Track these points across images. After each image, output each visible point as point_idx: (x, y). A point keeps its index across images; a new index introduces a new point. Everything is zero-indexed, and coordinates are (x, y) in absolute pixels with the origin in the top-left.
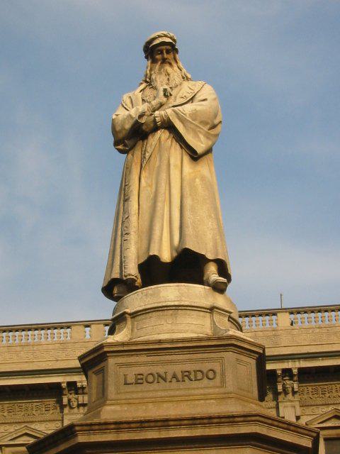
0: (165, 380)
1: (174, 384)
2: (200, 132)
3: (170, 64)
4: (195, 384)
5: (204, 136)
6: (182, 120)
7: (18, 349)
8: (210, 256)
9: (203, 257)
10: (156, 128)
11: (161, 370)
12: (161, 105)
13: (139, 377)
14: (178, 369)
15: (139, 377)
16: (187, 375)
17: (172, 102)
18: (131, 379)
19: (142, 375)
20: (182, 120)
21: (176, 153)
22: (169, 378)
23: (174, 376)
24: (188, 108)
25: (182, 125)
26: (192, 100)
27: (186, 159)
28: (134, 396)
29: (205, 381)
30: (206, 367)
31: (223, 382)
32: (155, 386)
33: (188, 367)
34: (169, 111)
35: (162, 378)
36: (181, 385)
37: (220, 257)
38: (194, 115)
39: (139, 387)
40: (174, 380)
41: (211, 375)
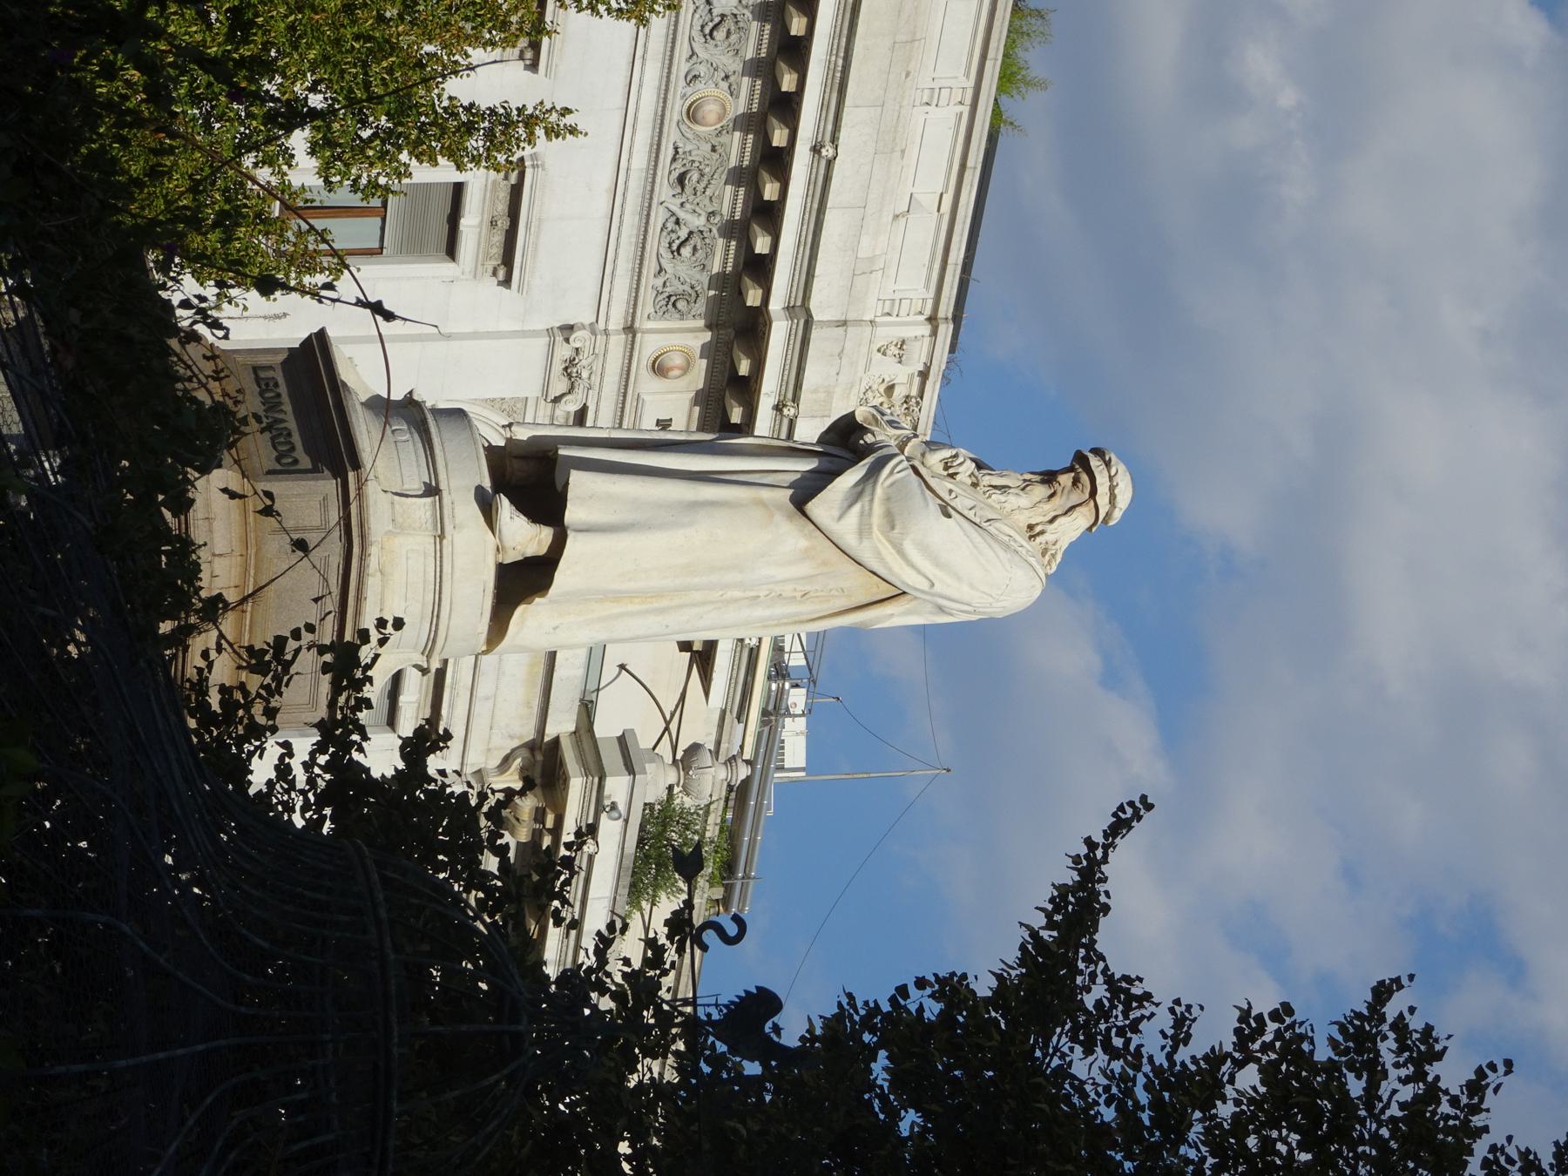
18: (262, 375)
29: (275, 454)
31: (269, 472)
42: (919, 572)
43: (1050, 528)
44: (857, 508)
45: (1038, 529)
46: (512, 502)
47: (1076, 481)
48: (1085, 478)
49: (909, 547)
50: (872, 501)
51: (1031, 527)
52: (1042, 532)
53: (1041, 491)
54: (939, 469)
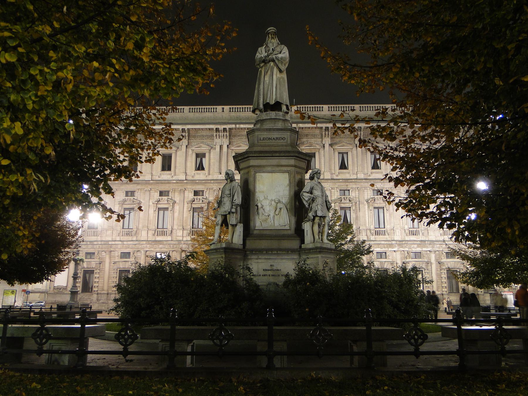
1: (274, 141)
4: (279, 141)
6: (278, 60)
10: (269, 61)
12: (271, 53)
14: (275, 137)
16: (277, 138)
17: (275, 52)
18: (262, 139)
20: (278, 60)
21: (275, 70)
23: (274, 138)
24: (280, 56)
26: (280, 53)
27: (278, 72)
32: (268, 141)
34: (274, 57)
36: (276, 141)
38: (282, 58)
39: (264, 141)
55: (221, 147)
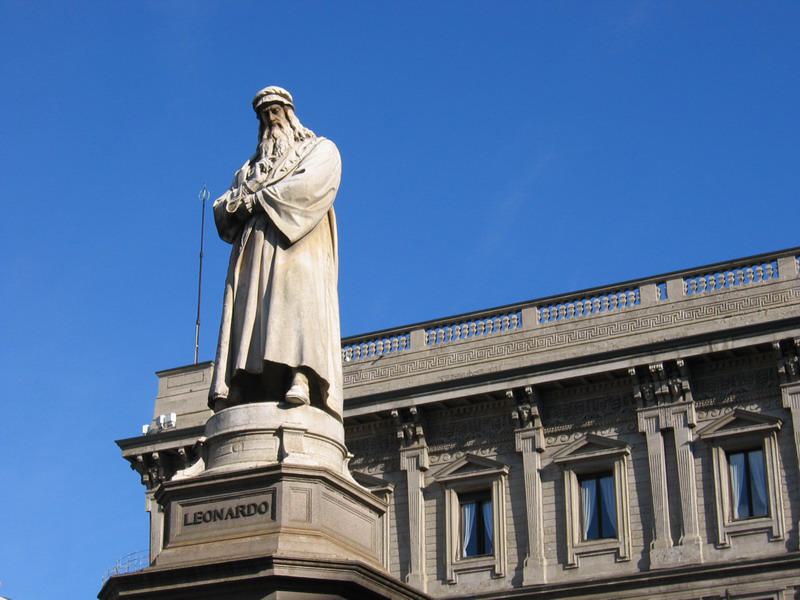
0: (221, 518)
2: (296, 214)
3: (280, 126)
5: (301, 215)
7: (570, 327)
8: (292, 363)
9: (285, 367)
11: (218, 506)
13: (199, 515)
14: (233, 504)
15: (199, 515)
18: (191, 519)
19: (201, 513)
22: (225, 512)
25: (273, 210)
28: (193, 537)
29: (258, 515)
30: (258, 500)
31: (273, 517)
32: (212, 524)
33: (245, 501)
35: (217, 515)
37: (304, 364)
40: (229, 516)
41: (263, 508)
42: (325, 195)
43: (297, 129)
44: (294, 216)
45: (297, 136)
46: (289, 388)
47: (275, 112)
48: (274, 106)
49: (318, 194)
50: (292, 208)
51: (296, 139)
52: (300, 134)
53: (276, 131)
54: (265, 176)
55: (668, 433)
